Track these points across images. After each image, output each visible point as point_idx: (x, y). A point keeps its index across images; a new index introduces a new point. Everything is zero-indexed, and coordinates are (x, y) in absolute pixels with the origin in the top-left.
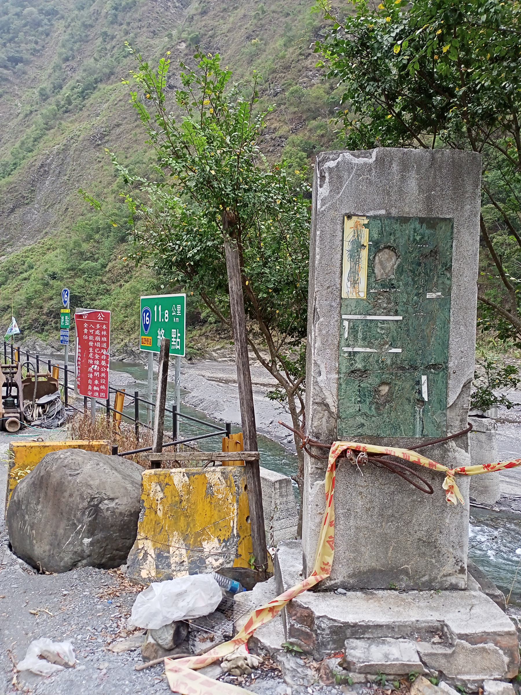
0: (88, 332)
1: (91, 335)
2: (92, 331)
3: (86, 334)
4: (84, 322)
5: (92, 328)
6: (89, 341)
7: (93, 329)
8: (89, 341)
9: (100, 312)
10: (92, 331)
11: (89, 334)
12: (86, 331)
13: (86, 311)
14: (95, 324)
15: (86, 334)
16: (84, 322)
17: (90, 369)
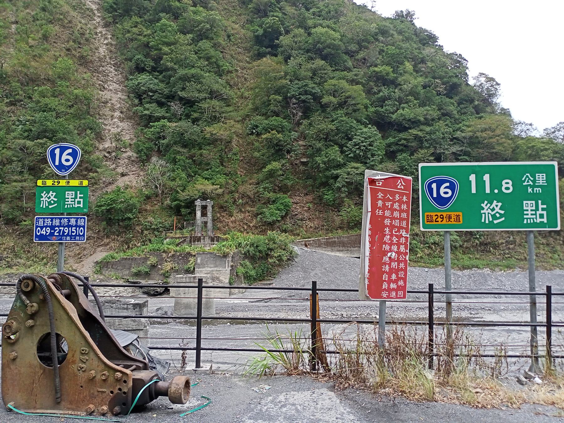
0: (384, 205)
1: (388, 209)
2: (389, 204)
3: (380, 208)
4: (378, 191)
5: (389, 200)
6: (384, 217)
7: (390, 201)
8: (384, 217)
9: (399, 178)
10: (389, 204)
11: (384, 208)
12: (380, 203)
13: (381, 175)
14: (393, 194)
15: (380, 208)
16: (378, 191)
17: (385, 259)
